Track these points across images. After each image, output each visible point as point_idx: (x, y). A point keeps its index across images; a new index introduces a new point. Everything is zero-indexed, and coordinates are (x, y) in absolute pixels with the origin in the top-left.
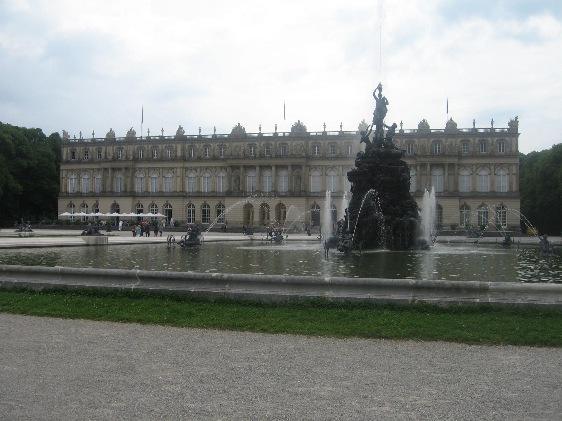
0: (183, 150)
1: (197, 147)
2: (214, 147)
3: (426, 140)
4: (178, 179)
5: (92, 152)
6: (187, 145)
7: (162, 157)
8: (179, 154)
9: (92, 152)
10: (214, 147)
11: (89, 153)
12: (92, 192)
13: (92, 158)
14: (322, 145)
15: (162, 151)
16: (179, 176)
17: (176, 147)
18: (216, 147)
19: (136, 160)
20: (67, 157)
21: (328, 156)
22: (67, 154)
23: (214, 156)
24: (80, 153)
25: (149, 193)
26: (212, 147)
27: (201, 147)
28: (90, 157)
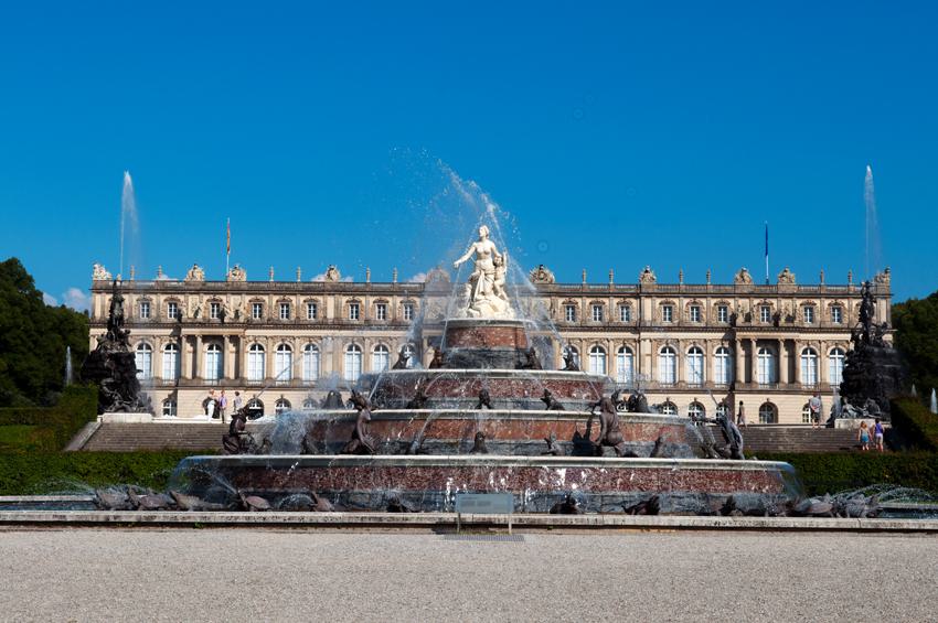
0: (337, 307)
1: (364, 302)
2: (394, 305)
3: (747, 300)
4: (330, 357)
5: (158, 305)
6: (344, 299)
7: (298, 318)
8: (331, 315)
9: (158, 305)
10: (394, 305)
11: (151, 306)
12: (157, 378)
13: (158, 316)
14: (580, 304)
15: (297, 307)
16: (330, 353)
17: (326, 303)
18: (398, 304)
19: (249, 324)
20: (103, 312)
21: (590, 324)
22: (103, 307)
23: (394, 319)
24: (131, 307)
25: (275, 380)
26: (390, 304)
27: (371, 304)
28: (153, 313)
